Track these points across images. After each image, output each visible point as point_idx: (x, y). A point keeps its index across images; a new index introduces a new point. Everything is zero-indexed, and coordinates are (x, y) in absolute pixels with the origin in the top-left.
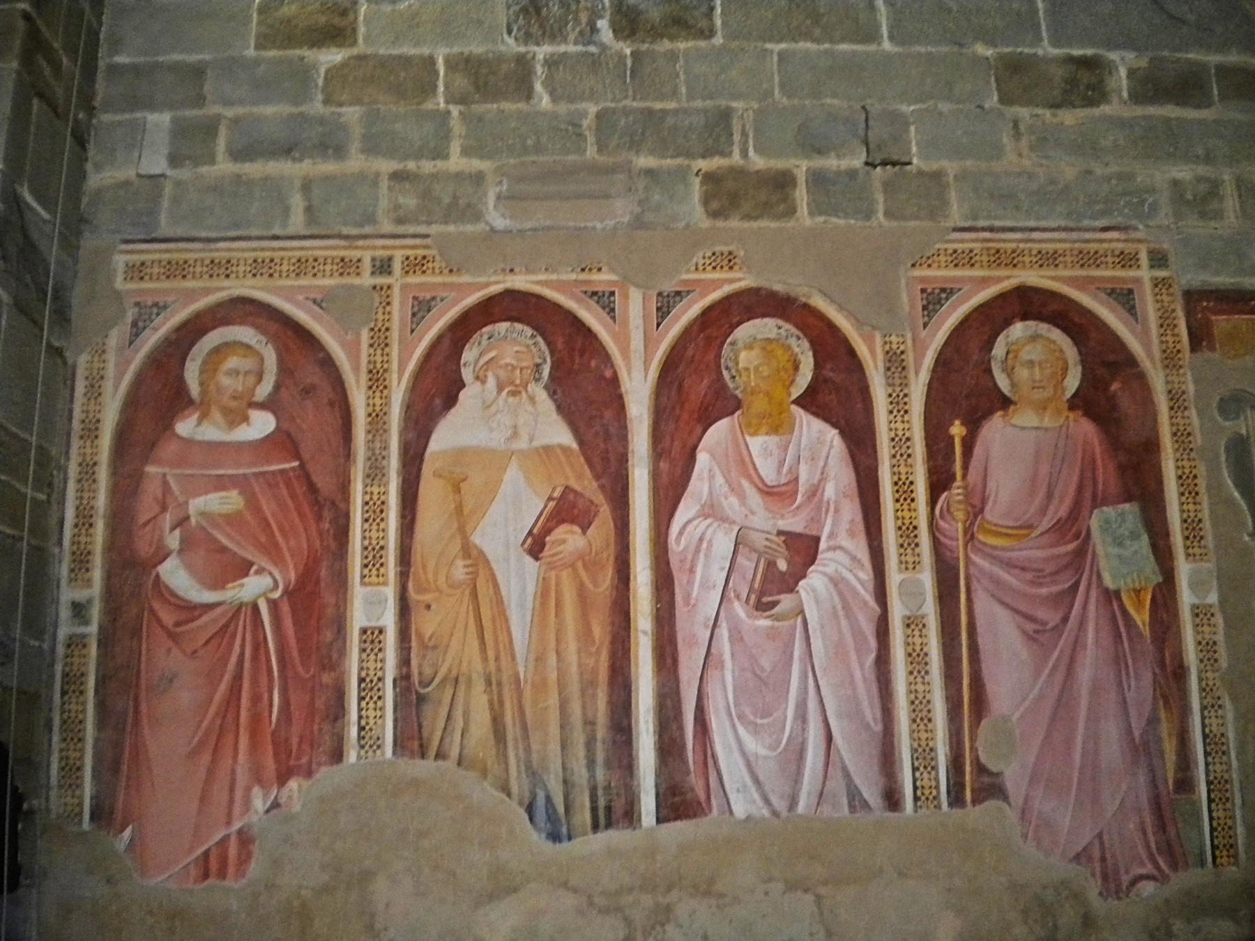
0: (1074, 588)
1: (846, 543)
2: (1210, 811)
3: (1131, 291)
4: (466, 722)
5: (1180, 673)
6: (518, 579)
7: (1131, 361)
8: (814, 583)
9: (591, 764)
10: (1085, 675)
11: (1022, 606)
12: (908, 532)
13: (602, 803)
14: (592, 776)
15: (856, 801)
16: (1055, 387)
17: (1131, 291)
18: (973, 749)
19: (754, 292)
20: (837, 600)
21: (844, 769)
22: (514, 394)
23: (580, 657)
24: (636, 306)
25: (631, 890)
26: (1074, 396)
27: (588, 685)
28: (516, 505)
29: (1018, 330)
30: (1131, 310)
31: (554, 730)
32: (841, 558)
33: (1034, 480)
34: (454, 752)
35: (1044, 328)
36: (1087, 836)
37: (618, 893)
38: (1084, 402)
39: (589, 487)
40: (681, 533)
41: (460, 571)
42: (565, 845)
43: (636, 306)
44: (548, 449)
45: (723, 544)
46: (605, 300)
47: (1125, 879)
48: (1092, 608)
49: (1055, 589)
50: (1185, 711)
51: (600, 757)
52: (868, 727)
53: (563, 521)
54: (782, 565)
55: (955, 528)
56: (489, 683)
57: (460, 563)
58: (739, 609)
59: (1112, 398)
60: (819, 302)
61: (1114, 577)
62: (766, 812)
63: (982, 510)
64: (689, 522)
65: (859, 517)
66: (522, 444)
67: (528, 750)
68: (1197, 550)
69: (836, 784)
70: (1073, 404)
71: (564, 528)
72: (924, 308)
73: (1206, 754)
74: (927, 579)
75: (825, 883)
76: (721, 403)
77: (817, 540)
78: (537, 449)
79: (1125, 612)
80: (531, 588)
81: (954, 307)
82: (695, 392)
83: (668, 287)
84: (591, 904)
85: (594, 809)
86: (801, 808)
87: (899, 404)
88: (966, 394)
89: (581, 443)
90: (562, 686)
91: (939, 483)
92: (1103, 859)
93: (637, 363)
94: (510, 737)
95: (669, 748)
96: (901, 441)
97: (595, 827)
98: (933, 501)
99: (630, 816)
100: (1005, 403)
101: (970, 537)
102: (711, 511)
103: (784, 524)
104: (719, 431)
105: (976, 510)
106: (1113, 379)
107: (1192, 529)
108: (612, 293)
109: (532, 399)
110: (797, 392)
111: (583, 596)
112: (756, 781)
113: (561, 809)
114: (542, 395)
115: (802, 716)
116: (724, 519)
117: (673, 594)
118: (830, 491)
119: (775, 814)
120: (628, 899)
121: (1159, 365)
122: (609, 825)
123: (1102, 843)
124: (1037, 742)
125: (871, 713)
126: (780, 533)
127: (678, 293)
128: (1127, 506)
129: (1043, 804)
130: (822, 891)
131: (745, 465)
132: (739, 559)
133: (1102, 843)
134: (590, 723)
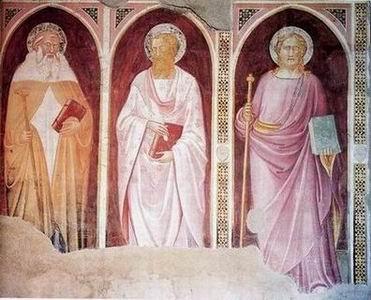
0: (297, 155)
1: (196, 130)
2: (354, 258)
3: (344, 11)
4: (26, 198)
5: (345, 196)
6: (50, 140)
7: (338, 47)
8: (180, 146)
9: (79, 220)
10: (298, 194)
11: (272, 161)
12: (223, 125)
13: (83, 237)
14: (79, 226)
15: (192, 242)
16: (299, 60)
17: (344, 11)
18: (245, 222)
19: (160, 10)
20: (189, 155)
21: (188, 229)
22: (49, 57)
23: (75, 175)
24: (107, 15)
25: (93, 274)
26: (308, 64)
27: (78, 187)
28: (49, 108)
29: (285, 31)
30: (343, 21)
31: (64, 205)
32: (193, 135)
33: (284, 103)
34: (21, 213)
35: (297, 30)
36: (295, 263)
37: (90, 274)
38: (311, 67)
39: (82, 100)
40: (122, 122)
41: (25, 136)
42: (67, 254)
43: (107, 15)
44: (65, 83)
45: (140, 127)
46: (93, 13)
47: (311, 285)
48: (305, 163)
49: (291, 153)
50: (346, 212)
51: (83, 219)
52: (198, 210)
53: (69, 116)
54: (166, 138)
55: (244, 125)
56: (37, 185)
57: (25, 133)
58: (146, 157)
59: (327, 67)
60: (191, 16)
61: (317, 149)
62: (153, 245)
63: (258, 116)
64: (126, 117)
65: (202, 118)
66: (53, 80)
67: (52, 213)
68: (360, 139)
69: (184, 234)
70: (308, 67)
71: (72, 118)
72: (241, 19)
73: (355, 232)
74: (230, 146)
75: (176, 276)
76: (142, 63)
77: (182, 127)
78: (60, 83)
79: (321, 166)
80: (56, 144)
81: (255, 19)
82: (132, 57)
83: (122, 8)
84: (77, 279)
85: (80, 240)
86: (167, 244)
87: (224, 66)
88: (256, 60)
89: (80, 80)
90: (68, 187)
91: (240, 102)
92: (301, 275)
93: (106, 44)
94: (45, 208)
95: (113, 216)
96: (223, 84)
97: (80, 247)
98: (236, 112)
99: (94, 243)
100: (275, 66)
101: (252, 129)
102: (135, 113)
103: (168, 120)
104: (141, 78)
105: (255, 118)
106: (328, 55)
107: (359, 129)
108: (96, 10)
109: (58, 59)
110: (177, 59)
111: (78, 151)
112: (150, 232)
113: (66, 240)
114: (63, 58)
115: (171, 200)
116: (141, 117)
117: (117, 149)
118: (189, 106)
119: (157, 246)
120: (92, 278)
121: (353, 48)
122: (86, 247)
123: (301, 269)
124: (275, 220)
125: (201, 205)
126: (166, 124)
127: (126, 10)
128: (328, 117)
129: (275, 248)
130: (175, 279)
131: (152, 92)
132: (147, 135)
133: (301, 269)
134: (78, 203)
